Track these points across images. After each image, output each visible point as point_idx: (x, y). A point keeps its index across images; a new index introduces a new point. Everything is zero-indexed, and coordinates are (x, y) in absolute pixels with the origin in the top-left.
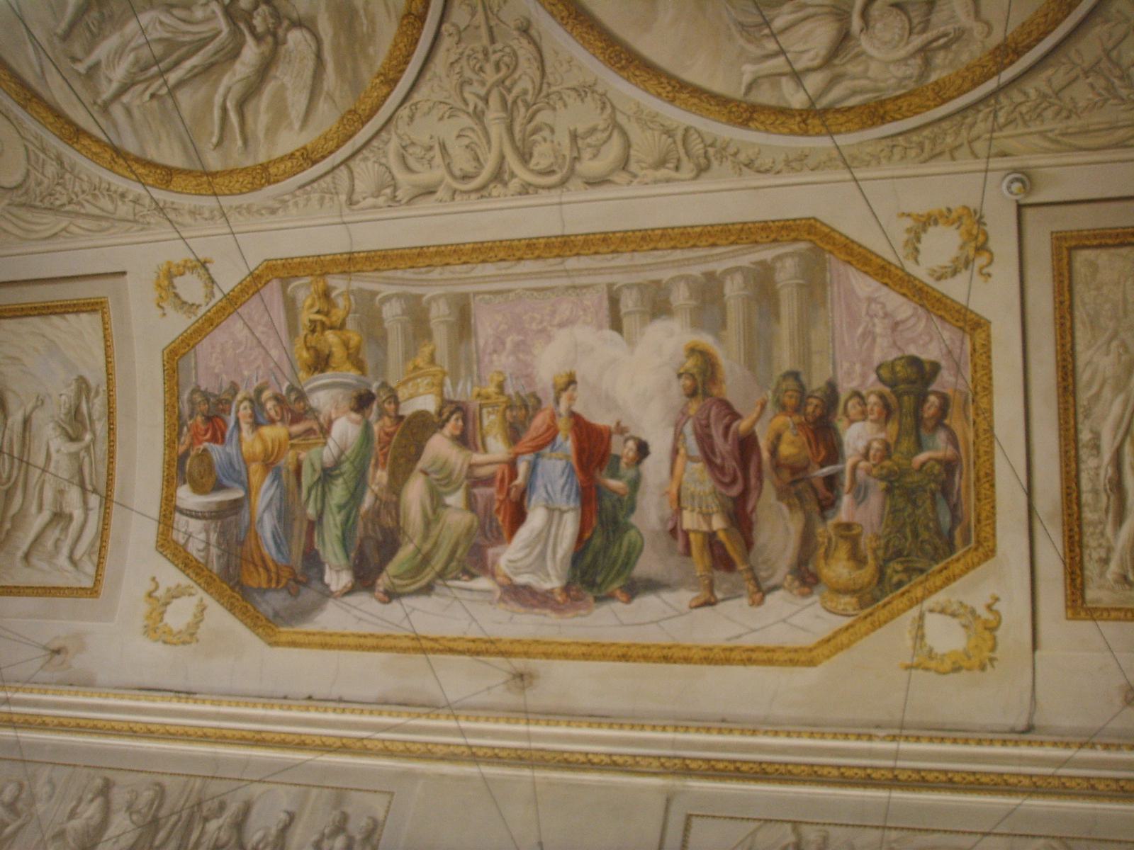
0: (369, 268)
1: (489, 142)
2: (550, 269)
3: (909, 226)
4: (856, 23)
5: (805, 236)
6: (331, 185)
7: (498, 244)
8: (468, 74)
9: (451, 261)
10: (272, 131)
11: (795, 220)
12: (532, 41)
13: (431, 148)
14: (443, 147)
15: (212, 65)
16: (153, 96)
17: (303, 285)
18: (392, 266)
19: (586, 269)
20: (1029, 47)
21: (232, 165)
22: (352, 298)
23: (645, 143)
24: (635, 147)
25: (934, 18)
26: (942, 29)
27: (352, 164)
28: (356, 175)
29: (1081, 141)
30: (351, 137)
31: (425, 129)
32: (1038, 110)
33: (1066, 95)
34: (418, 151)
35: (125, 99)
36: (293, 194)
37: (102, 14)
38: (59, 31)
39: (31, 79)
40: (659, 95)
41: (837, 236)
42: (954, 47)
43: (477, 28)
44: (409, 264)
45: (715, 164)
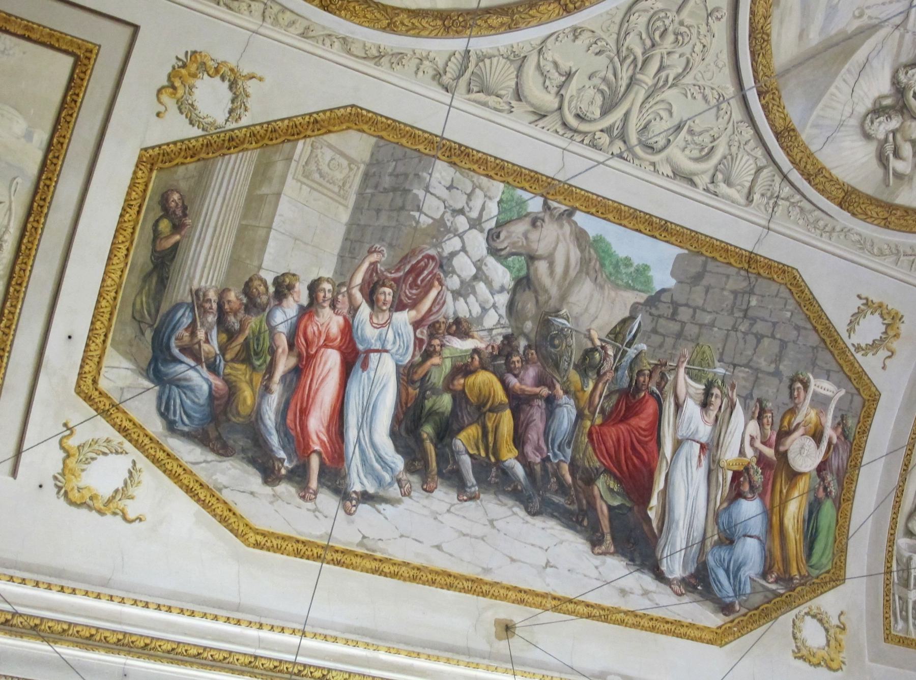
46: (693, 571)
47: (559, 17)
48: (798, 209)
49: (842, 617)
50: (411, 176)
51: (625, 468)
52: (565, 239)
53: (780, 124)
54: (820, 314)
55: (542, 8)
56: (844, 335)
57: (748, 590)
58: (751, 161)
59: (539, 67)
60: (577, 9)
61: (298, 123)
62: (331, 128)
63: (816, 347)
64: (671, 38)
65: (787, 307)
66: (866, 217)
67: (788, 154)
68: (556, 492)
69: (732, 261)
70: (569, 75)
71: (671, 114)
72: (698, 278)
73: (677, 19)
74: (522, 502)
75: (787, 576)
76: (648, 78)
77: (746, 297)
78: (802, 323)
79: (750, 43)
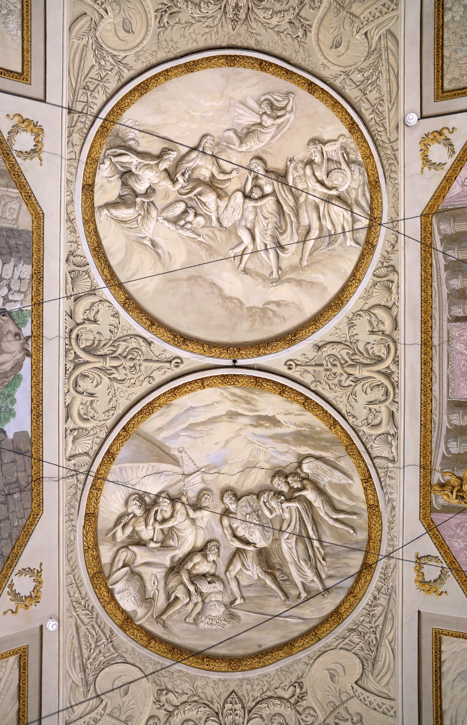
0: (430, 458)
1: (370, 377)
2: (438, 353)
3: (427, 169)
4: (334, 192)
5: (430, 219)
6: (383, 470)
7: (423, 381)
8: (335, 381)
9: (430, 408)
10: (351, 497)
11: (421, 224)
12: (324, 345)
13: (370, 409)
14: (370, 403)
15: (313, 519)
16: (324, 559)
17: (436, 500)
18: (429, 443)
19: (439, 333)
20: (352, 118)
21: (366, 526)
22: (445, 471)
23: (379, 297)
24: (380, 302)
25: (335, 159)
26: (340, 156)
27: (373, 456)
28: (379, 455)
29: (394, 94)
30: (359, 453)
31: (361, 411)
32: (379, 113)
33: (373, 102)
34: (370, 417)
35: (323, 576)
36: (385, 494)
37: (279, 569)
38: (283, 598)
39: (304, 628)
40: (357, 287)
41: (431, 203)
42: (348, 150)
43: (315, 371)
44: (429, 433)
45: (392, 263)
47: (119, 302)
48: (74, 491)
50: (19, 255)
52: (14, 357)
53: (114, 448)
54: (23, 546)
55: (120, 292)
56: (16, 571)
58: (90, 446)
59: (93, 304)
60: (126, 310)
61: (26, 187)
62: (29, 205)
63: (3, 556)
64: (131, 364)
65: (20, 521)
66: (85, 536)
67: (101, 465)
69: (34, 468)
70: (95, 322)
71: (96, 386)
72: (18, 452)
73: (141, 362)
76: (110, 363)
77: (17, 490)
78: (14, 537)
79: (145, 406)
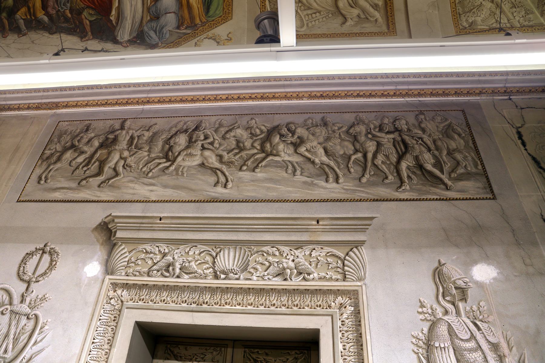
46: (135, 35)
49: (230, 35)
51: (97, 3)
57: (168, 35)
68: (64, 22)
74: (46, 30)
75: (193, 25)
